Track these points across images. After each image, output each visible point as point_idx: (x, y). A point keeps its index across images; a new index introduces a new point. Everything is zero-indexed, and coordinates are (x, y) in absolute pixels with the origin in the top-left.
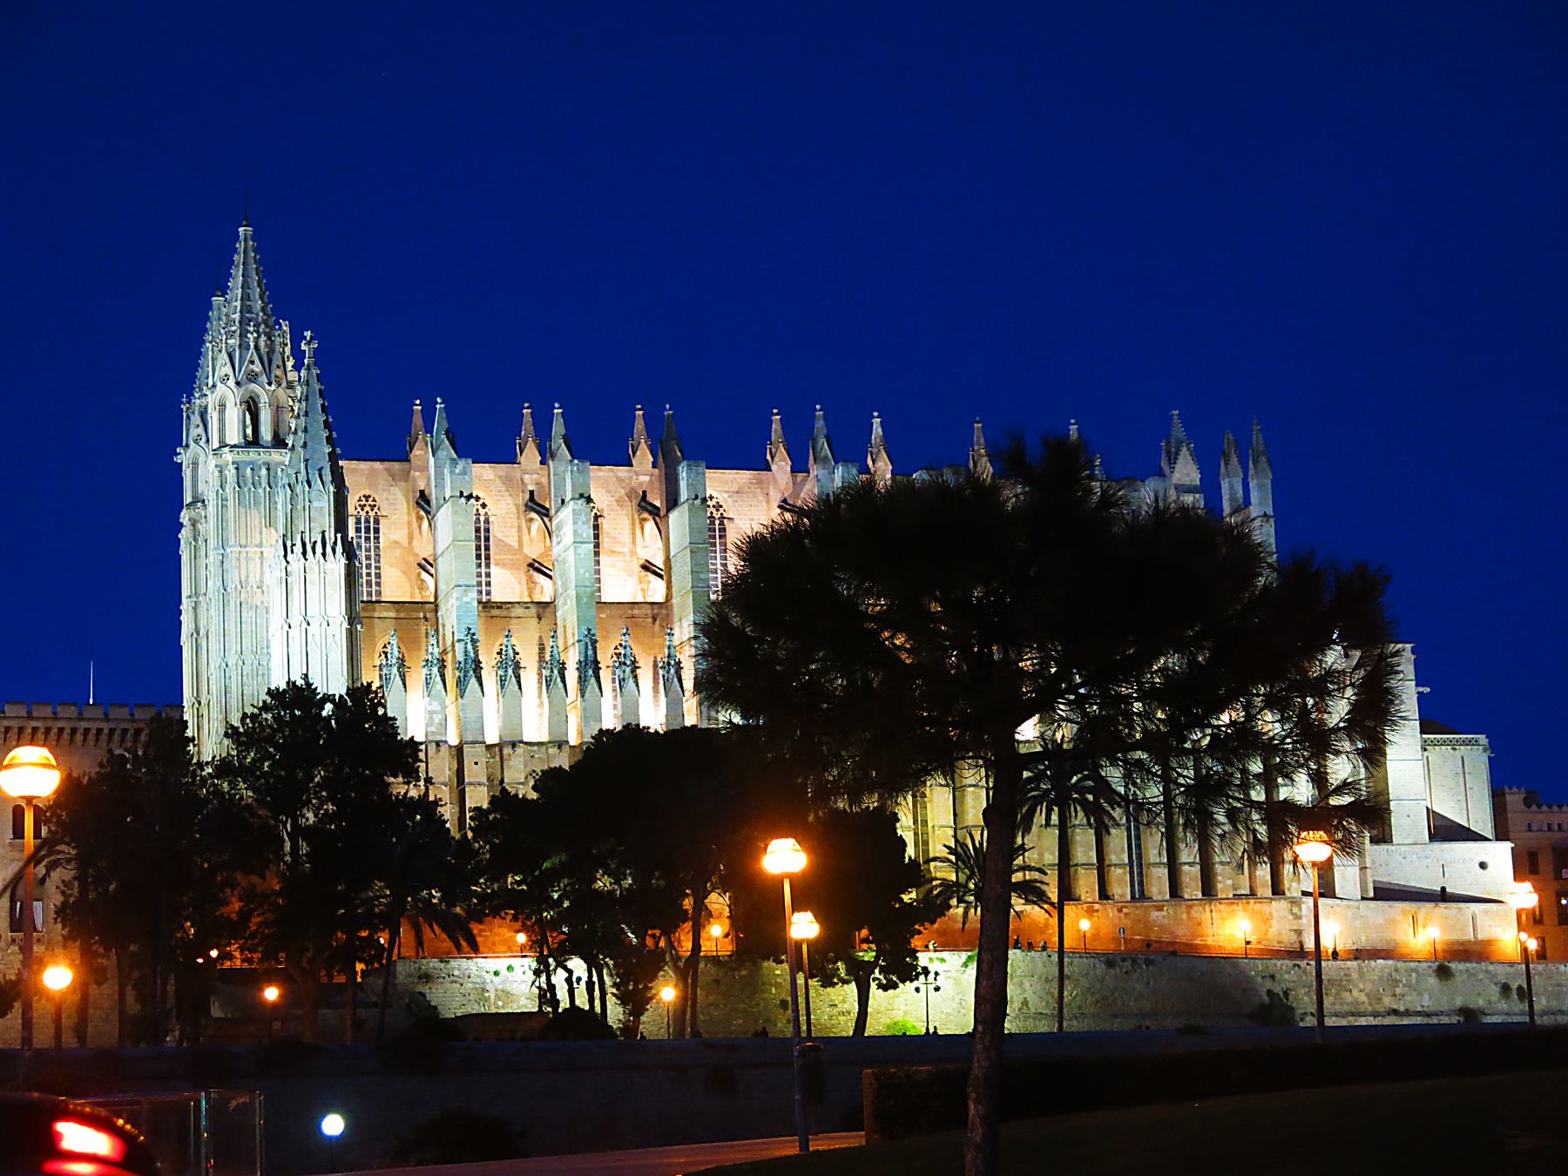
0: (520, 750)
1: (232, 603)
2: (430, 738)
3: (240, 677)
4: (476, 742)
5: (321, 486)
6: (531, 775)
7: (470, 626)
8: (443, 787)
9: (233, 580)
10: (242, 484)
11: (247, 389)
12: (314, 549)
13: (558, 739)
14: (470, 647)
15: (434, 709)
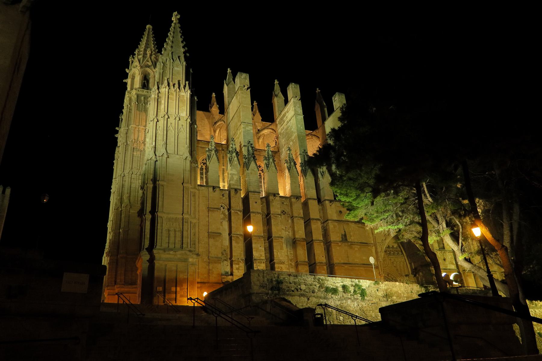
0: (278, 198)
1: (130, 148)
2: (232, 187)
3: (130, 179)
4: (256, 192)
5: (179, 62)
6: (282, 213)
7: (250, 141)
8: (239, 213)
9: (132, 137)
10: (139, 101)
11: (145, 70)
12: (174, 85)
13: (296, 195)
14: (250, 149)
15: (234, 173)
